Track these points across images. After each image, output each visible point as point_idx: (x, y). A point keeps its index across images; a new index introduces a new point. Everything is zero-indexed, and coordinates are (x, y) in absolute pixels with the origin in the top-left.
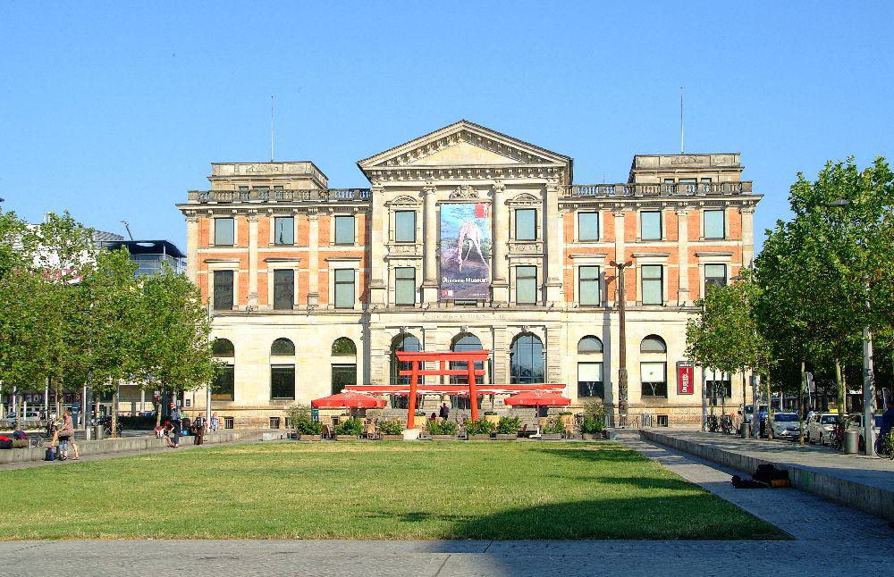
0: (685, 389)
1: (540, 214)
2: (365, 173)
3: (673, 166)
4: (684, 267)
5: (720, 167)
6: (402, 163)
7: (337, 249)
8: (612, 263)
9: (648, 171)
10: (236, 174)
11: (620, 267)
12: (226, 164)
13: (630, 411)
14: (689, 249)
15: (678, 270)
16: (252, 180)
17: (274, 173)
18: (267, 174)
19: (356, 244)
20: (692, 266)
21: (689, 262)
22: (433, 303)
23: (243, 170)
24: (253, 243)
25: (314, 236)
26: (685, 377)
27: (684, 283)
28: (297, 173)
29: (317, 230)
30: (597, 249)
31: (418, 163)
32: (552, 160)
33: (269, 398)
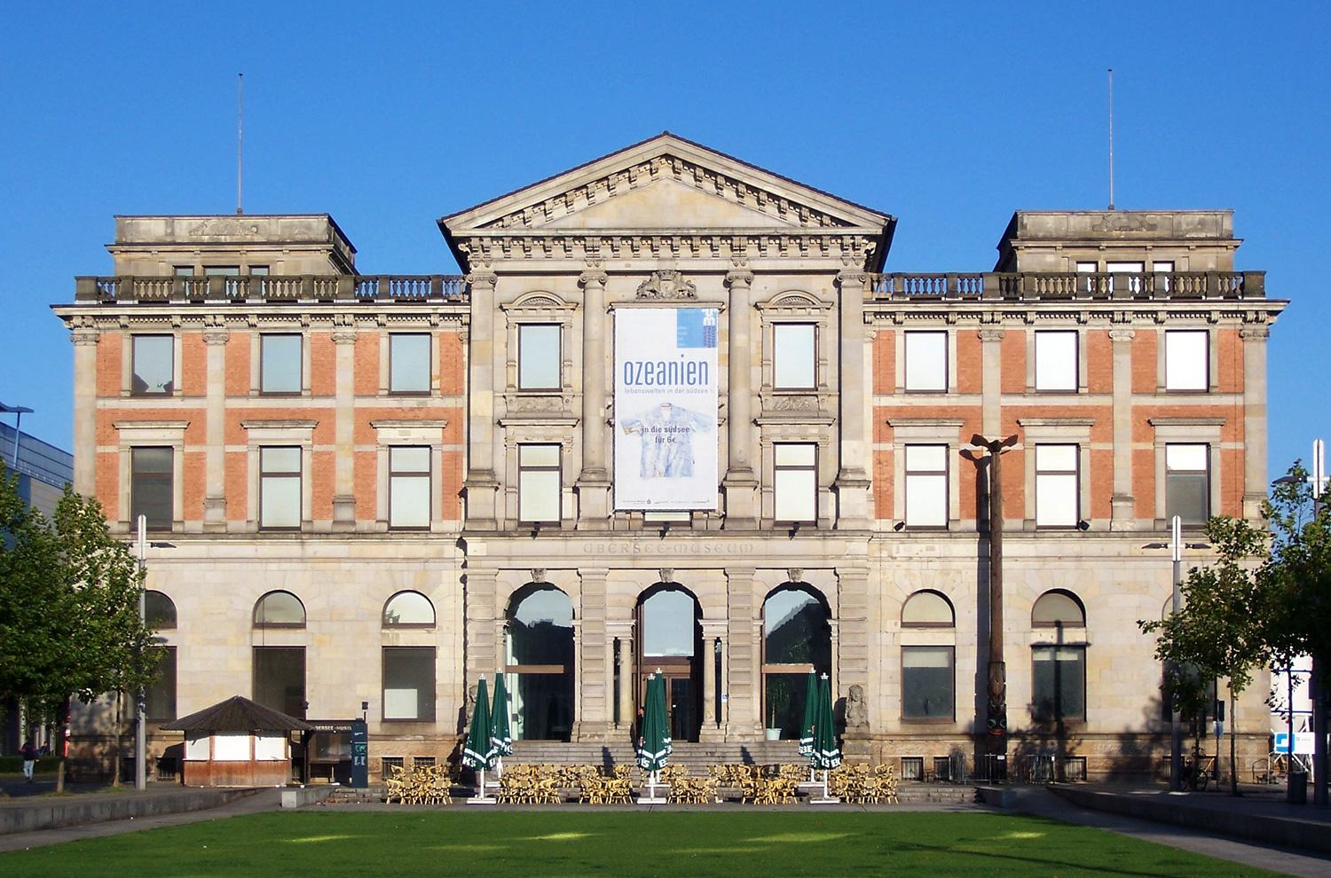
1: (830, 336)
2: (453, 242)
3: (1095, 235)
4: (1124, 450)
6: (535, 222)
7: (393, 403)
9: (1047, 240)
10: (169, 239)
11: (994, 447)
12: (150, 217)
14: (1137, 411)
15: (1111, 454)
17: (248, 238)
18: (235, 239)
20: (1142, 446)
21: (1137, 439)
23: (183, 228)
24: (215, 388)
25: (345, 377)
27: (1123, 482)
28: (299, 237)
29: (350, 362)
31: (572, 222)
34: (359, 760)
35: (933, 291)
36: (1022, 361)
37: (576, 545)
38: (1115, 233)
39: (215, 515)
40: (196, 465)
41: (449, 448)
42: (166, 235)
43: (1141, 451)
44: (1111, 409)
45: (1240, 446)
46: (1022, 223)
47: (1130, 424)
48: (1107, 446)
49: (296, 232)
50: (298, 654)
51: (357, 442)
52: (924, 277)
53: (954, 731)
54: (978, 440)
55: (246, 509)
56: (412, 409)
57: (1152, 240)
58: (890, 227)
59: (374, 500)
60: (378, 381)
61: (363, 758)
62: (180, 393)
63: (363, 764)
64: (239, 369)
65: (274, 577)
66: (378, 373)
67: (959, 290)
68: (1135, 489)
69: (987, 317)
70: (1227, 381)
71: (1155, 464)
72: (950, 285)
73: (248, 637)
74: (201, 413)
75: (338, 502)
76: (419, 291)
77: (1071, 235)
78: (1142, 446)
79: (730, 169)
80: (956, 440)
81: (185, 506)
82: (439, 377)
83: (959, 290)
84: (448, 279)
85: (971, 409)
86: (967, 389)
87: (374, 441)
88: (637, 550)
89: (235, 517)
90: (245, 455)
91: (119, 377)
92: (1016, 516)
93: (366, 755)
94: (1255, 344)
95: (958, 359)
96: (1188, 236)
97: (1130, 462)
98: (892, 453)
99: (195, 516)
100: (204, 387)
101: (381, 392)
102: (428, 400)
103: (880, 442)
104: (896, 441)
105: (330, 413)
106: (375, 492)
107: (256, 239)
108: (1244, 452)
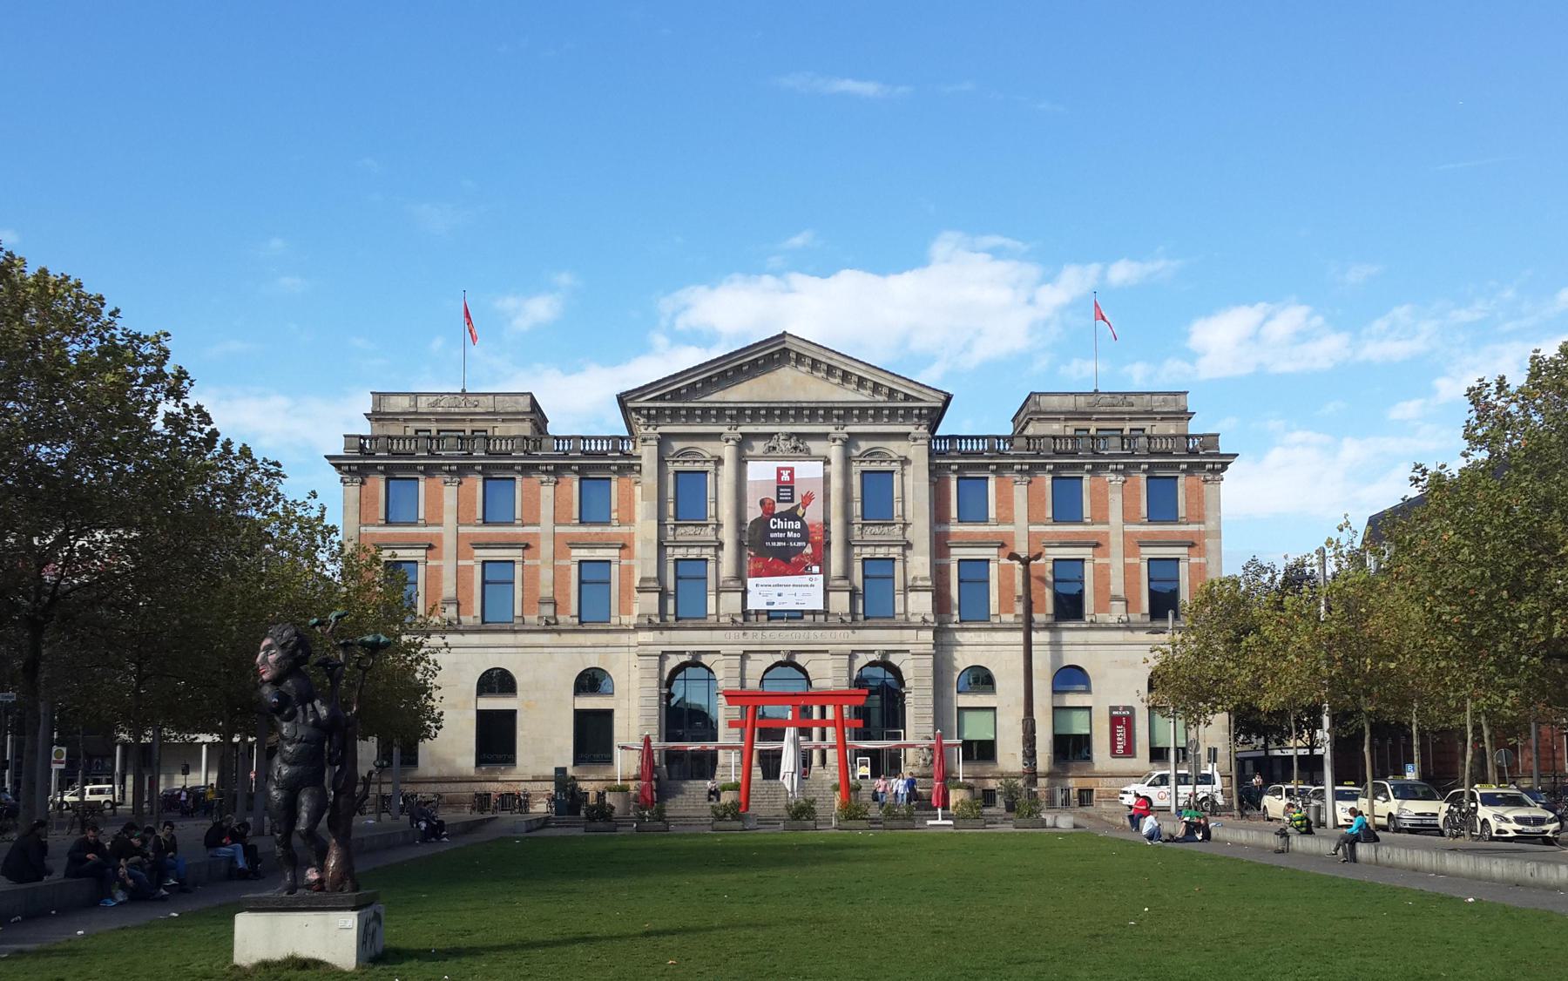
3: (1088, 410)
5: (1158, 413)
7: (583, 529)
8: (1013, 556)
10: (412, 410)
15: (1107, 566)
16: (437, 420)
17: (473, 410)
18: (462, 410)
19: (615, 523)
24: (449, 518)
25: (546, 511)
26: (1121, 730)
27: (1117, 587)
28: (509, 410)
30: (986, 534)
32: (921, 397)
33: (473, 764)
37: (718, 635)
38: (1102, 409)
39: (451, 611)
41: (624, 562)
44: (1107, 533)
48: (1128, 560)
50: (511, 715)
52: (972, 438)
53: (996, 769)
54: (1013, 556)
56: (597, 534)
57: (1129, 413)
60: (572, 513)
66: (571, 507)
69: (1017, 467)
72: (991, 443)
73: (474, 703)
74: (439, 536)
75: (542, 602)
76: (602, 447)
79: (831, 359)
80: (996, 557)
82: (617, 511)
83: (997, 447)
84: (622, 438)
86: (1004, 518)
87: (569, 556)
90: (472, 567)
91: (377, 509)
95: (996, 497)
96: (1155, 410)
100: (442, 517)
102: (608, 529)
104: (1142, 556)
105: (536, 536)
107: (478, 410)
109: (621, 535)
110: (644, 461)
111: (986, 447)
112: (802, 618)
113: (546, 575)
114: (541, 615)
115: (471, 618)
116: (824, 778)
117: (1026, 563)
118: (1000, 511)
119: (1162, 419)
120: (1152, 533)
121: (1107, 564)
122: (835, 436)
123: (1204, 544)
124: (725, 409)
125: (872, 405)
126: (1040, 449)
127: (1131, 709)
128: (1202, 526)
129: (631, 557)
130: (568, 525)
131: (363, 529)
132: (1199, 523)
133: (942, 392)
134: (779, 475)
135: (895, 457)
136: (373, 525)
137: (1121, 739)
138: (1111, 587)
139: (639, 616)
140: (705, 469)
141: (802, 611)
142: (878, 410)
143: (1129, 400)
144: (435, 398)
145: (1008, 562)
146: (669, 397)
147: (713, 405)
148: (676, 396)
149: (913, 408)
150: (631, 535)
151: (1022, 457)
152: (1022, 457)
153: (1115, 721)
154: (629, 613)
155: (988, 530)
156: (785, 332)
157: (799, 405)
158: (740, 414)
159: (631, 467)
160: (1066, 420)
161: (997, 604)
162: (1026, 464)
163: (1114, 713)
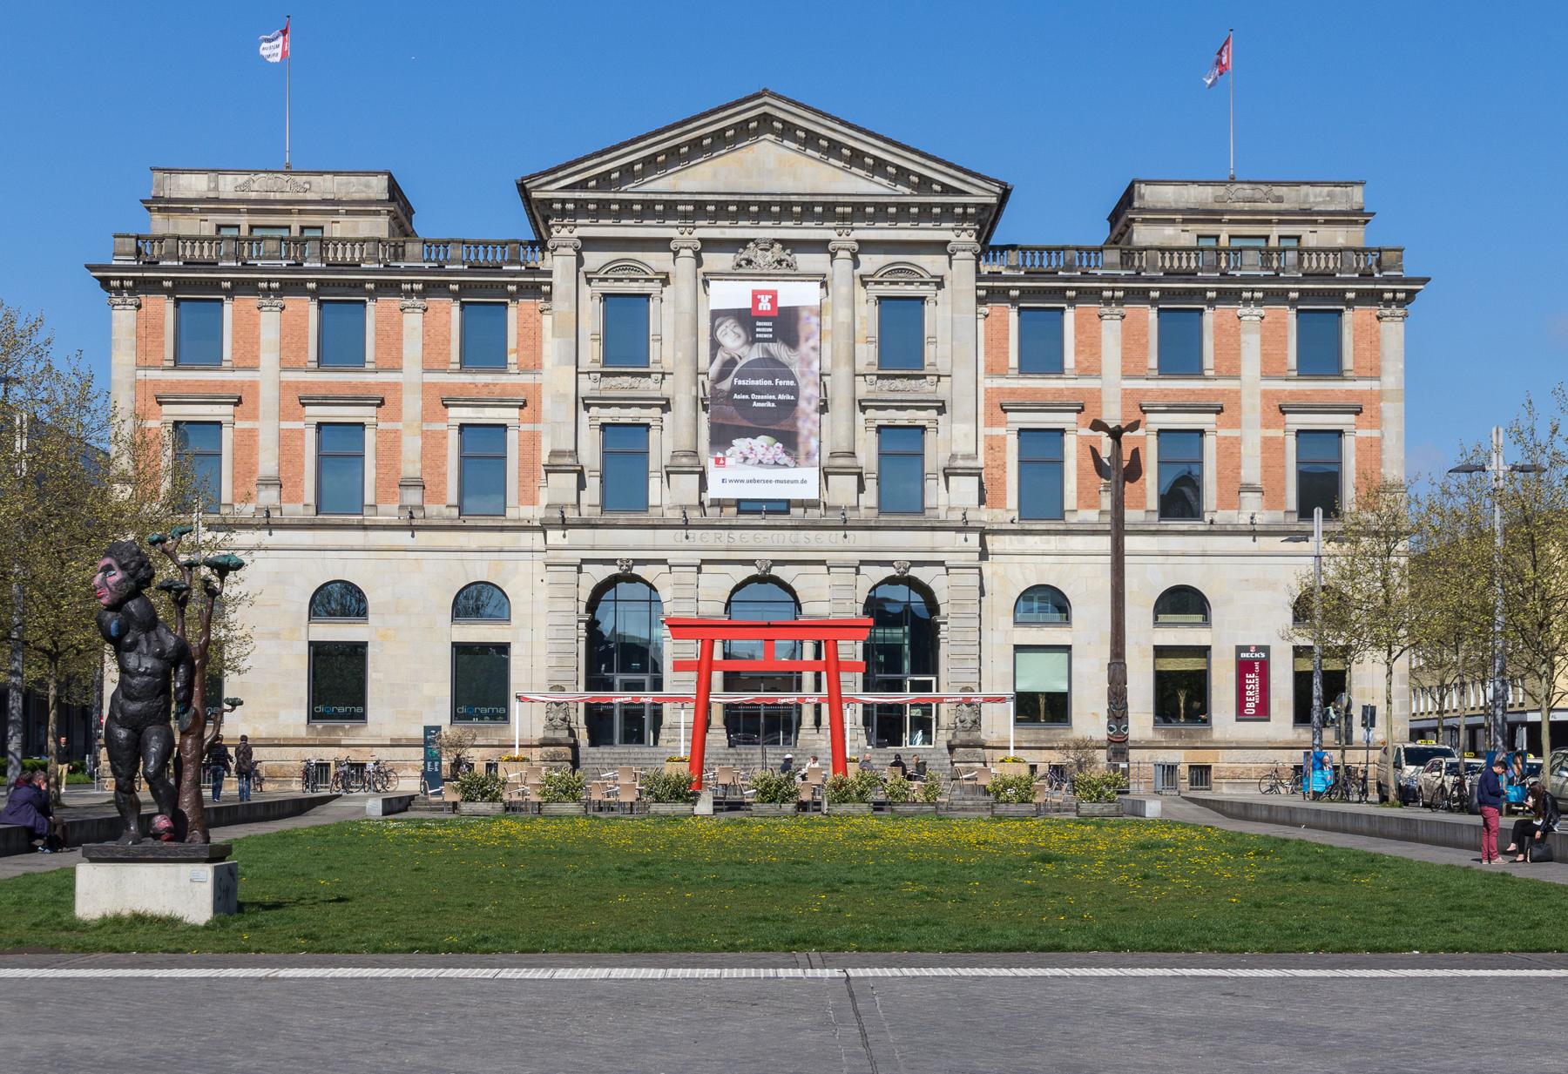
0: (1250, 706)
3: (1217, 206)
5: (1320, 213)
8: (1097, 425)
9: (1163, 216)
10: (212, 195)
11: (1116, 434)
12: (191, 171)
13: (1134, 755)
14: (1266, 394)
15: (1237, 441)
16: (250, 212)
17: (301, 196)
18: (286, 196)
19: (513, 369)
20: (1271, 433)
22: (691, 507)
23: (228, 186)
24: (269, 359)
25: (412, 349)
26: (1252, 680)
27: (1251, 471)
28: (357, 196)
30: (1060, 392)
34: (433, 765)
35: (1050, 265)
36: (1143, 341)
38: (1239, 206)
39: (268, 497)
40: (247, 441)
41: (525, 427)
42: (209, 190)
43: (1271, 439)
44: (1238, 393)
45: (1375, 433)
46: (1139, 192)
47: (1259, 409)
49: (354, 189)
51: (424, 419)
54: (1097, 425)
55: (303, 491)
56: (486, 385)
58: (1005, 195)
59: (444, 482)
61: (436, 763)
62: (230, 364)
63: (436, 770)
64: (296, 339)
65: (480, 570)
67: (1077, 264)
68: (1264, 478)
70: (1362, 364)
71: (1284, 452)
72: (1068, 258)
73: (304, 630)
74: (254, 386)
75: (405, 485)
77: (1192, 206)
78: (1271, 433)
81: (234, 487)
82: (517, 351)
85: (1090, 391)
86: (1085, 370)
87: (445, 418)
88: (731, 540)
89: (290, 500)
90: (302, 432)
91: (162, 345)
92: (1137, 507)
93: (440, 761)
94: (1393, 324)
96: (1316, 209)
97: (1258, 450)
98: (1004, 438)
99: (248, 498)
100: (257, 357)
101: (452, 366)
102: (503, 379)
103: (992, 425)
105: (396, 386)
106: (445, 474)
107: (309, 196)
108: (1380, 440)
109: (523, 387)
110: (556, 279)
111: (1062, 263)
112: (788, 512)
113: (411, 446)
114: (405, 504)
115: (300, 507)
116: (817, 746)
117: (1116, 434)
118: (1081, 358)
119: (1327, 222)
120: (1304, 393)
121: (1236, 438)
122: (838, 245)
123: (1379, 411)
124: (676, 203)
125: (893, 199)
126: (1140, 266)
127: (1266, 649)
128: (1377, 383)
129: (536, 419)
130: (444, 371)
131: (141, 373)
132: (1371, 378)
133: (997, 181)
134: (756, 301)
135: (927, 278)
136: (156, 368)
137: (1251, 694)
138: (1243, 472)
139: (548, 506)
140: (646, 291)
141: (788, 501)
142: (903, 208)
143: (1277, 194)
144: (246, 177)
145: (1091, 433)
146: (593, 183)
147: (658, 197)
148: (604, 181)
149: (954, 205)
150: (537, 388)
151: (1115, 279)
152: (1115, 279)
153: (1244, 667)
154: (534, 502)
155: (1064, 386)
156: (765, 90)
157: (785, 198)
158: (700, 209)
159: (537, 286)
160: (1185, 221)
161: (1075, 494)
162: (1120, 289)
163: (1243, 655)
